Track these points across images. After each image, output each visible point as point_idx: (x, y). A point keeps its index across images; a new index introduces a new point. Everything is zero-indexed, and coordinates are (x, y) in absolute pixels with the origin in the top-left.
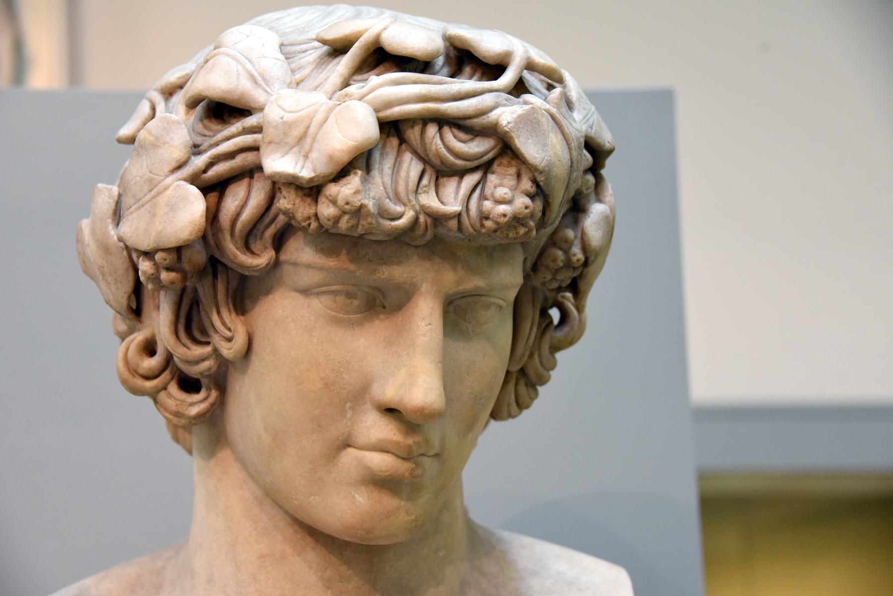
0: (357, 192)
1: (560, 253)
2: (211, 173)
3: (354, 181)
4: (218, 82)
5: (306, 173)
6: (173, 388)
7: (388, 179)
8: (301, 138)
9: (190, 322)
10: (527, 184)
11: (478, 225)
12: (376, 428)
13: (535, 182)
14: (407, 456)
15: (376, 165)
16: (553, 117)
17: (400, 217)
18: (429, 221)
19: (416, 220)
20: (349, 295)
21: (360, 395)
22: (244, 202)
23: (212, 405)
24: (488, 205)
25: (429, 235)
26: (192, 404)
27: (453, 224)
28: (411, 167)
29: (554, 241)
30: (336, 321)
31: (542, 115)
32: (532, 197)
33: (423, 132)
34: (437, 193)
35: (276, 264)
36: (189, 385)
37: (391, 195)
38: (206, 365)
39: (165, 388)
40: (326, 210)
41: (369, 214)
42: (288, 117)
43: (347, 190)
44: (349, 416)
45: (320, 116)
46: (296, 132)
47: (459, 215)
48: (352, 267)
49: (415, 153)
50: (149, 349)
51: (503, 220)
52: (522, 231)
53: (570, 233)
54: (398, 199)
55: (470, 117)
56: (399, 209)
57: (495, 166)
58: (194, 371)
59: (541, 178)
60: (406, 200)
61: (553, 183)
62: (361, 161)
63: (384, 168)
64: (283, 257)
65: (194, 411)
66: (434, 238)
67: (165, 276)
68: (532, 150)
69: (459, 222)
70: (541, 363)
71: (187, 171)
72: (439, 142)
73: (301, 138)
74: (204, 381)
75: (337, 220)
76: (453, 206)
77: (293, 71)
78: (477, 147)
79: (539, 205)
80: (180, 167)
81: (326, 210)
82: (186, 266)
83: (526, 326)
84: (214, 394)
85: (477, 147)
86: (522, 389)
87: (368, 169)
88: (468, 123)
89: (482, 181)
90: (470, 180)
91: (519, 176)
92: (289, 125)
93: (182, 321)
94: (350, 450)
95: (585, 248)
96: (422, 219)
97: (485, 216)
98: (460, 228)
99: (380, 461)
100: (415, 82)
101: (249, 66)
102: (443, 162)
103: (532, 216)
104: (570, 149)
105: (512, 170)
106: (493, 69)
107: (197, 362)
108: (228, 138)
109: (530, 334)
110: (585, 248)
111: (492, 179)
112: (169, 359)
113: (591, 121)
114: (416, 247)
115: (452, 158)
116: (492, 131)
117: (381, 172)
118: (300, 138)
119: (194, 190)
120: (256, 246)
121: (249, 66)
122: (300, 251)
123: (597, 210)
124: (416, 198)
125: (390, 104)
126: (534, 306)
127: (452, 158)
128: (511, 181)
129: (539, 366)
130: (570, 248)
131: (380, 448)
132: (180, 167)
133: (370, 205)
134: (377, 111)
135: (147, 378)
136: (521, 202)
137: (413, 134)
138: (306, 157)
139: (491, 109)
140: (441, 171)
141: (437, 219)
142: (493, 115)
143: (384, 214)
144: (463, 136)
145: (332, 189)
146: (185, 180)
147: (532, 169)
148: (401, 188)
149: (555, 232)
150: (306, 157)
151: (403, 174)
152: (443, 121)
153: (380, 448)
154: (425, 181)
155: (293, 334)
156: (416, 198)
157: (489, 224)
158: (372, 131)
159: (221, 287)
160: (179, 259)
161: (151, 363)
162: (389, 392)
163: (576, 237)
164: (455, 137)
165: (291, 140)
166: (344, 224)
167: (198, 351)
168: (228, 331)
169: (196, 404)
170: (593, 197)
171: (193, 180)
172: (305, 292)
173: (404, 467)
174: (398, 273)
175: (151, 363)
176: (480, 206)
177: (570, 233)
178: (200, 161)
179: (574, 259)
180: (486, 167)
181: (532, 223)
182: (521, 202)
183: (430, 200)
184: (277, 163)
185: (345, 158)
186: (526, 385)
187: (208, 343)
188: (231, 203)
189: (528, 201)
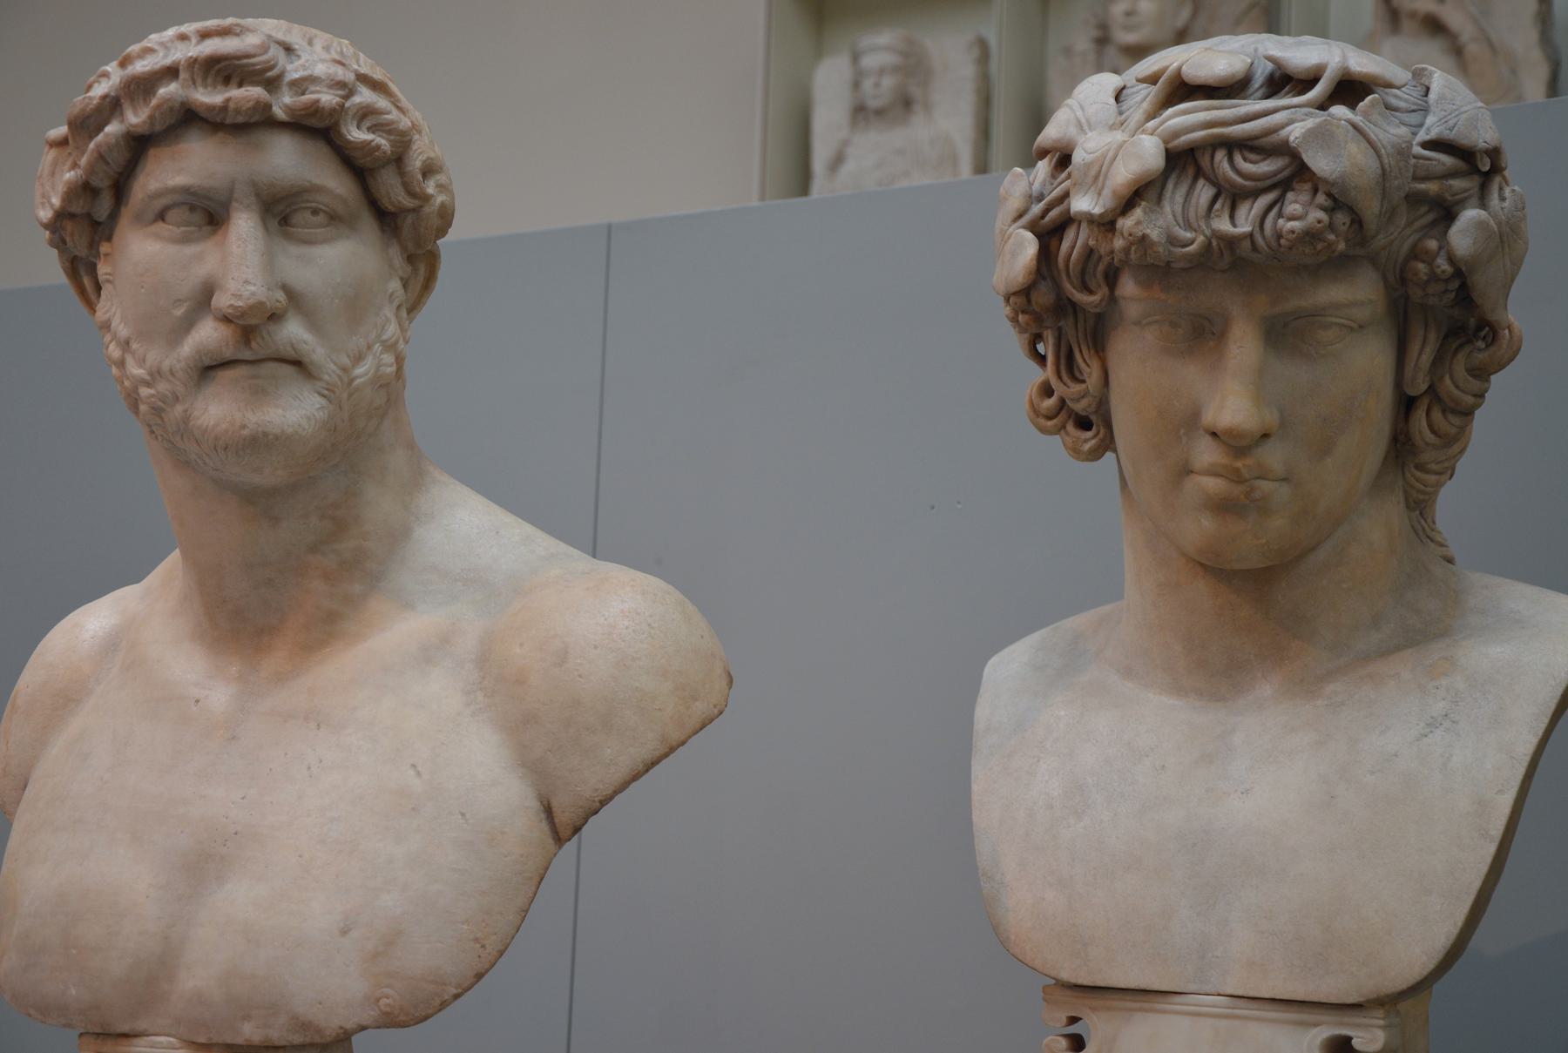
0: (1138, 223)
1: (1421, 266)
2: (1047, 219)
3: (1138, 213)
4: (1052, 132)
5: (1097, 210)
6: (1070, 427)
7: (1178, 209)
8: (1096, 178)
9: (1068, 365)
10: (1321, 198)
11: (1274, 244)
12: (1206, 453)
13: (1329, 195)
14: (1236, 477)
15: (1168, 194)
16: (1355, 127)
17: (1192, 243)
19: (1208, 247)
20: (1174, 325)
21: (1191, 421)
22: (1073, 244)
23: (1102, 440)
25: (1227, 258)
26: (1086, 441)
27: (1247, 244)
29: (1415, 254)
31: (1338, 126)
32: (1329, 211)
34: (1232, 217)
35: (1112, 299)
36: (1084, 424)
37: (1180, 219)
38: (1084, 402)
39: (1064, 427)
40: (1119, 243)
41: (1153, 244)
42: (1089, 158)
43: (1126, 223)
44: (1184, 439)
45: (1111, 154)
46: (1093, 173)
47: (1251, 235)
48: (1163, 296)
49: (1208, 179)
50: (1047, 390)
51: (1291, 236)
52: (1319, 246)
53: (1432, 244)
54: (1188, 226)
55: (1257, 138)
56: (1189, 235)
57: (1295, 185)
58: (1079, 407)
59: (1334, 191)
60: (1195, 225)
61: (1353, 193)
62: (1140, 193)
63: (1175, 197)
64: (1117, 293)
65: (1087, 447)
66: (1229, 260)
67: (1020, 317)
68: (1321, 163)
69: (1253, 242)
70: (1457, 387)
72: (1226, 165)
73: (1096, 178)
74: (1093, 418)
75: (1127, 250)
76: (1244, 226)
77: (1121, 113)
78: (1265, 167)
79: (1342, 219)
82: (1035, 307)
83: (1414, 347)
84: (1102, 431)
85: (1265, 167)
86: (1437, 415)
87: (1160, 199)
88: (1256, 143)
89: (1280, 200)
90: (1264, 201)
91: (1316, 191)
92: (1088, 166)
93: (1063, 361)
94: (1193, 476)
95: (1451, 260)
96: (1214, 243)
97: (1279, 236)
98: (1254, 247)
99: (1213, 485)
100: (1208, 109)
101: (1079, 113)
102: (1232, 184)
103: (1331, 227)
104: (1379, 156)
105: (1308, 186)
106: (1304, 82)
107: (1078, 400)
109: (1420, 354)
110: (1451, 260)
111: (1290, 196)
112: (1062, 402)
113: (1451, 123)
114: (1223, 271)
115: (1239, 180)
116: (1285, 150)
117: (1172, 198)
118: (1097, 175)
119: (1029, 235)
120: (1093, 286)
121: (1079, 113)
122: (1128, 287)
123: (1470, 215)
124: (1209, 226)
125: (1176, 134)
126: (1426, 326)
127: (1239, 180)
128: (1305, 197)
129: (1452, 388)
130: (1434, 259)
131: (1212, 472)
132: (1020, 216)
133: (1155, 234)
134: (1166, 142)
135: (1049, 418)
136: (1316, 215)
137: (1205, 161)
138: (1099, 194)
139: (1283, 126)
140: (1233, 196)
141: (1230, 242)
142: (1283, 133)
143: (1173, 241)
144: (1252, 156)
146: (1024, 227)
147: (1326, 181)
148: (1192, 214)
149: (1415, 245)
150: (1099, 194)
151: (1194, 201)
152: (1232, 146)
153: (1212, 472)
154: (1217, 206)
155: (1137, 369)
156: (1209, 226)
159: (1081, 325)
160: (1029, 301)
161: (1050, 403)
162: (1209, 417)
163: (1440, 248)
164: (1245, 159)
165: (1089, 180)
167: (1076, 388)
169: (1089, 440)
170: (1475, 200)
171: (1033, 227)
173: (1238, 490)
175: (1050, 403)
176: (1275, 223)
177: (1432, 244)
178: (1037, 209)
179: (1438, 271)
180: (1283, 185)
181: (1332, 237)
182: (1316, 215)
183: (1223, 225)
184: (1082, 204)
185: (1127, 193)
186: (1444, 412)
187: (1084, 381)
188: (1065, 245)
189: (1321, 215)
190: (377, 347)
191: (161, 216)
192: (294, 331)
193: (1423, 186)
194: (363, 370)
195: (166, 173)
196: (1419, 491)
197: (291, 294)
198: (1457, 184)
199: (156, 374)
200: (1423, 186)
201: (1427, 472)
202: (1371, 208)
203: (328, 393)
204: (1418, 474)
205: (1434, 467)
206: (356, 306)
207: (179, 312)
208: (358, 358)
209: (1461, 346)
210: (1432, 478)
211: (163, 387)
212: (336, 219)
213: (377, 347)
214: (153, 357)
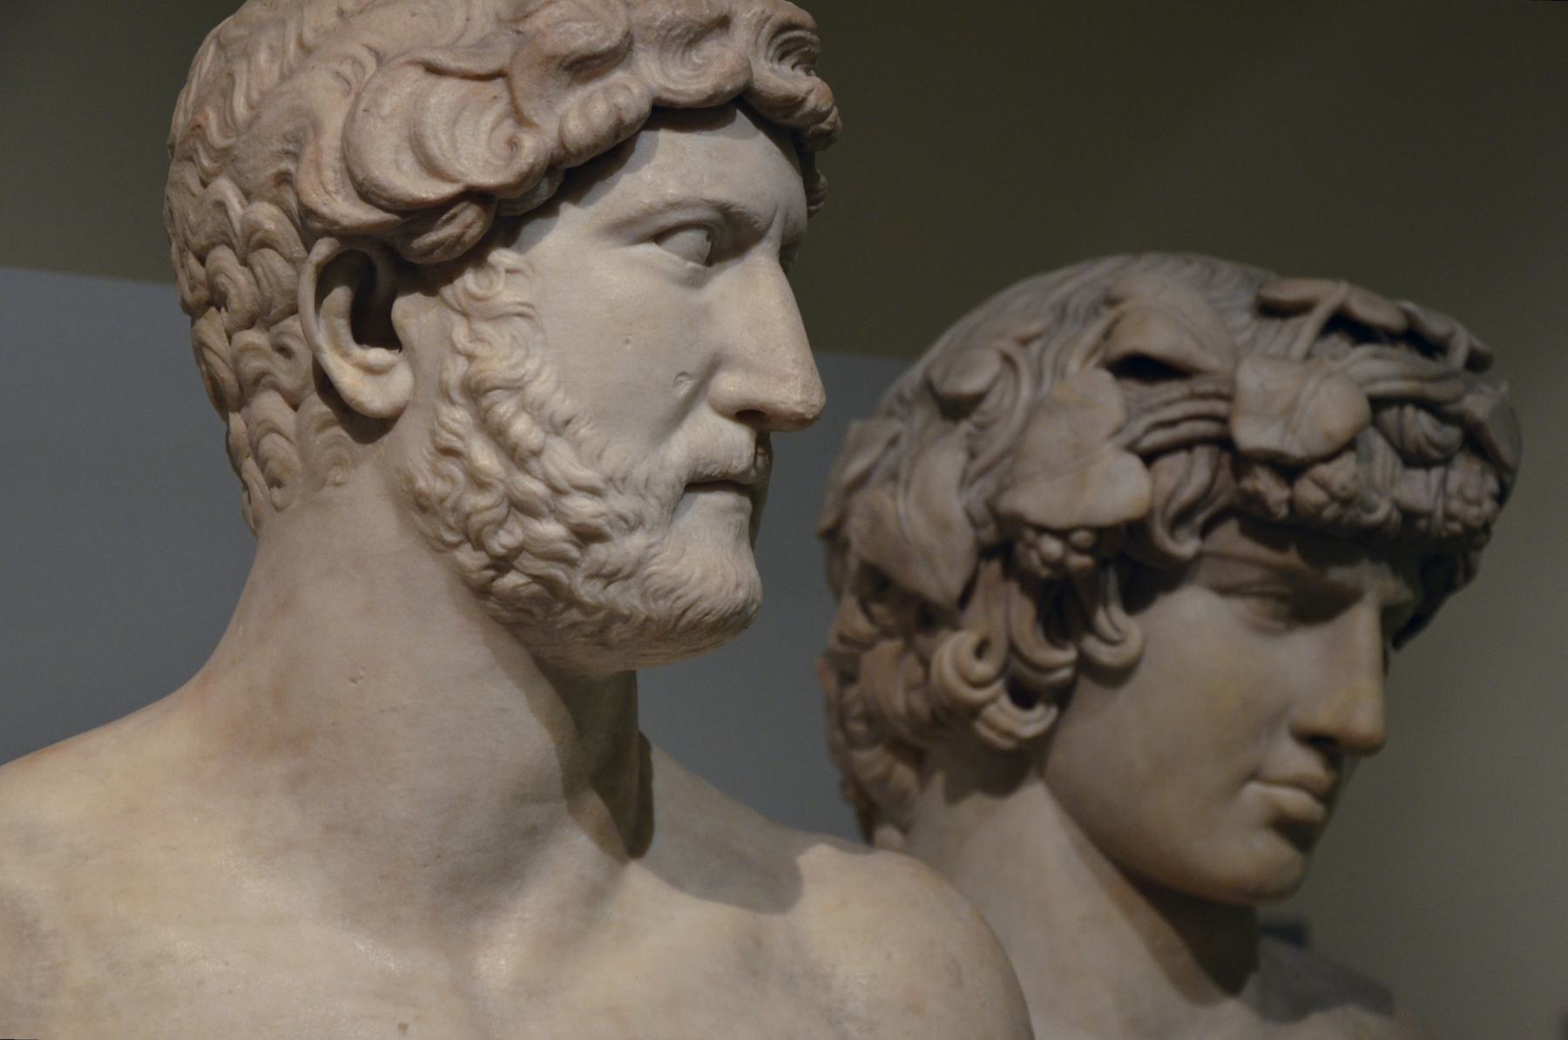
6: (1005, 701)
18: (1396, 516)
20: (1281, 598)
24: (1456, 506)
26: (1028, 723)
28: (1383, 456)
30: (1259, 629)
33: (1401, 416)
40: (1308, 492)
43: (1341, 473)
71: (1126, 438)
80: (1118, 431)
81: (1308, 492)
94: (1254, 788)
108: (1168, 404)
120: (1183, 533)
125: (1374, 380)
131: (1297, 784)
141: (1409, 516)
145: (1323, 471)
153: (1297, 784)
157: (1456, 527)
158: (1362, 409)
166: (1330, 512)
168: (1120, 631)
171: (1131, 448)
172: (1225, 591)
174: (1338, 575)
191: (659, 237)
195: (672, 170)
199: (617, 482)
207: (685, 388)
211: (623, 503)
214: (618, 455)
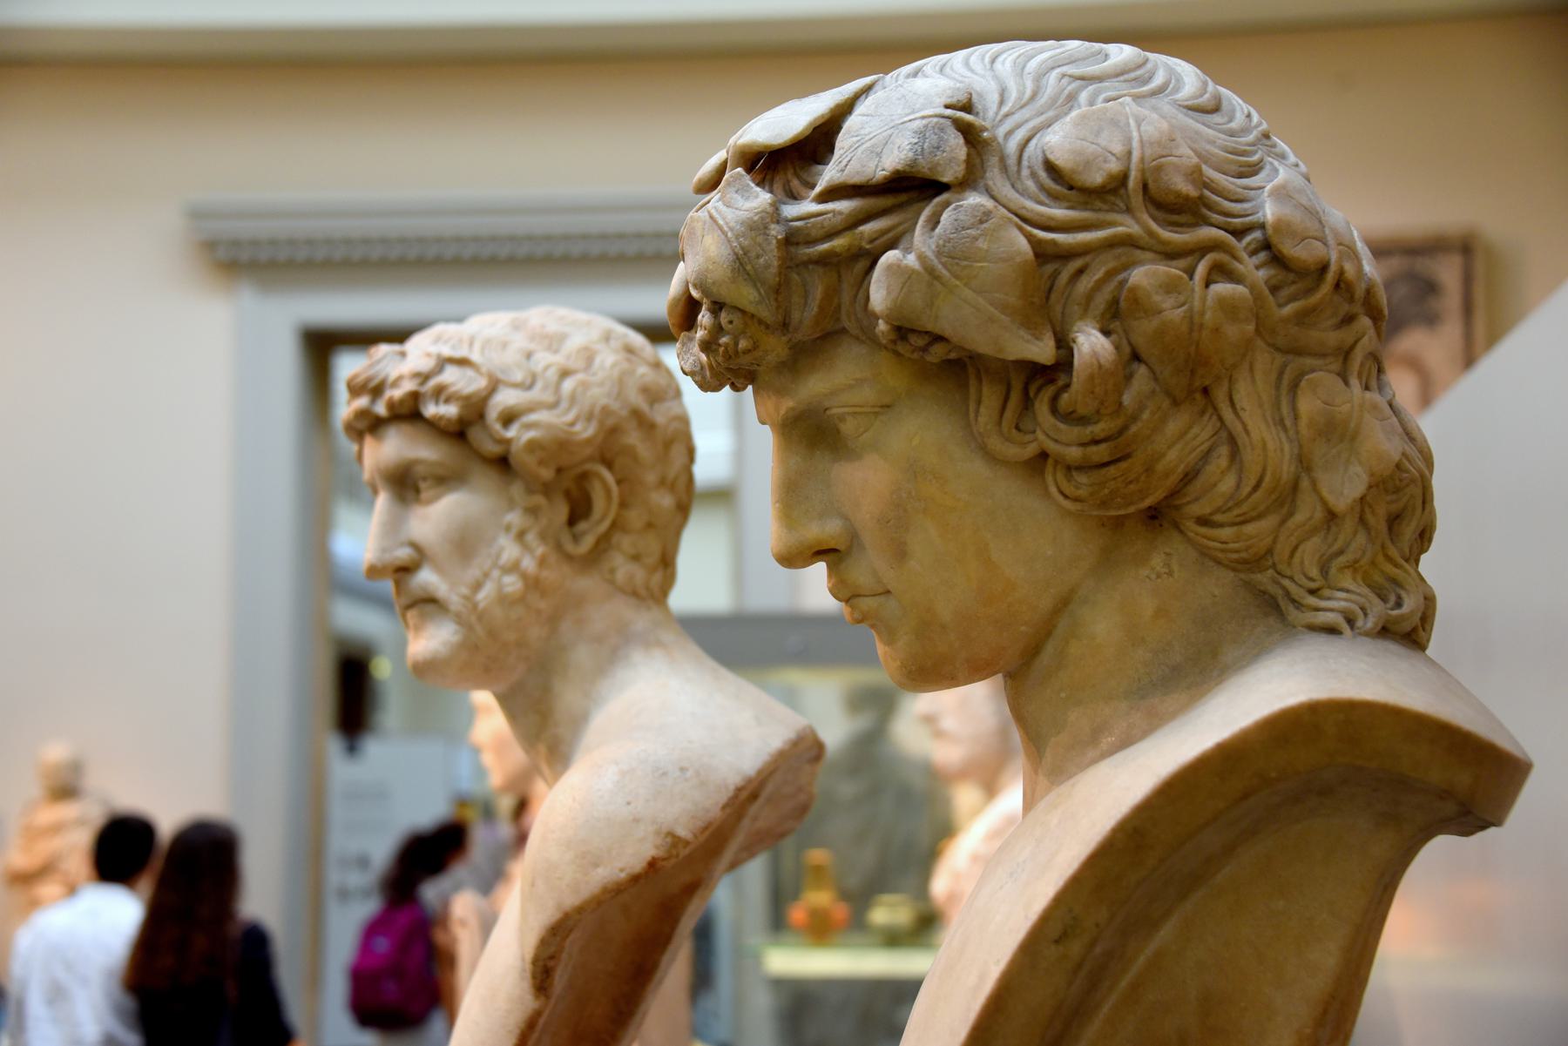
126: (980, 380)
190: (496, 573)
192: (427, 578)
193: (825, 246)
194: (485, 595)
196: (1222, 551)
197: (415, 546)
198: (868, 228)
200: (825, 246)
201: (1221, 525)
202: (747, 296)
203: (459, 619)
204: (1203, 530)
205: (1219, 518)
206: (465, 544)
208: (477, 586)
209: (1039, 390)
210: (1226, 533)
212: (445, 480)
213: (496, 573)
